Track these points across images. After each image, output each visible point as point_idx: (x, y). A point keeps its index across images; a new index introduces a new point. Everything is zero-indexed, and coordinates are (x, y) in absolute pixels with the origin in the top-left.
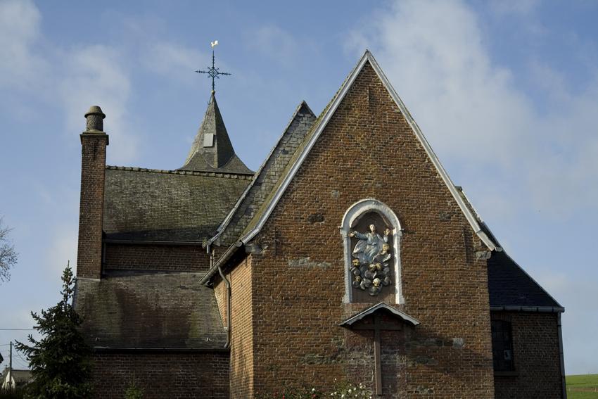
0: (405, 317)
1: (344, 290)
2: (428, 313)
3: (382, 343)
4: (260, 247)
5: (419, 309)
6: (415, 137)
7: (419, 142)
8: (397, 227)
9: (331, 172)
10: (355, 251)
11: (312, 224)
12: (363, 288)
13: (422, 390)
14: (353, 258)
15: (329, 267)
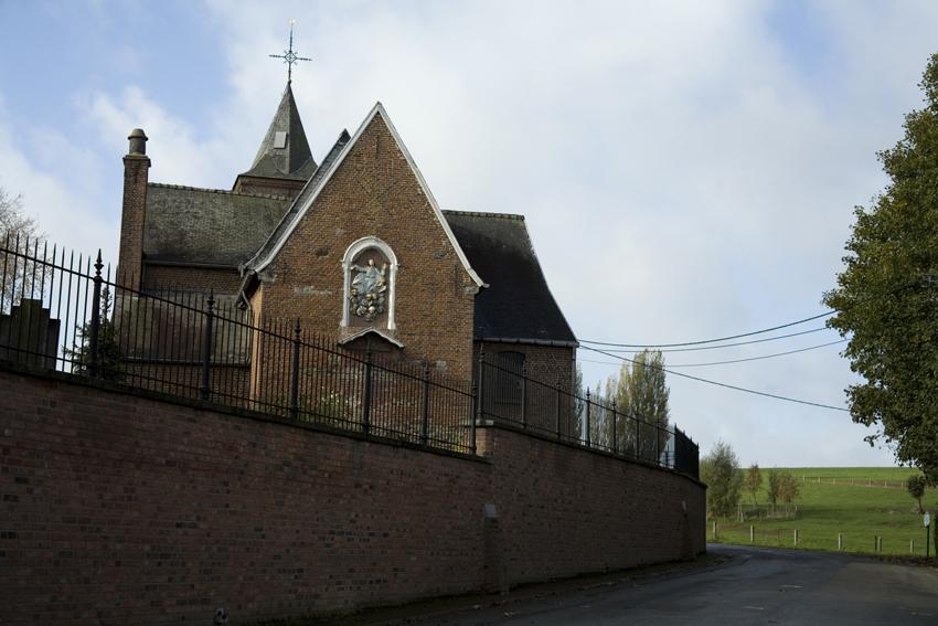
0: (392, 341)
14: (352, 288)
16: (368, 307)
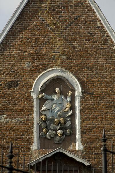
0: (78, 159)
1: (33, 139)
5: (95, 154)
6: (96, 16)
7: (100, 21)
8: (78, 89)
9: (25, 48)
10: (43, 109)
11: (9, 89)
12: (49, 138)
14: (41, 114)
15: (21, 122)
16: (56, 131)
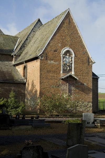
0: (76, 78)
2: (79, 77)
3: (69, 83)
4: (42, 57)
10: (64, 60)
13: (77, 95)
14: (63, 62)
16: (67, 68)
